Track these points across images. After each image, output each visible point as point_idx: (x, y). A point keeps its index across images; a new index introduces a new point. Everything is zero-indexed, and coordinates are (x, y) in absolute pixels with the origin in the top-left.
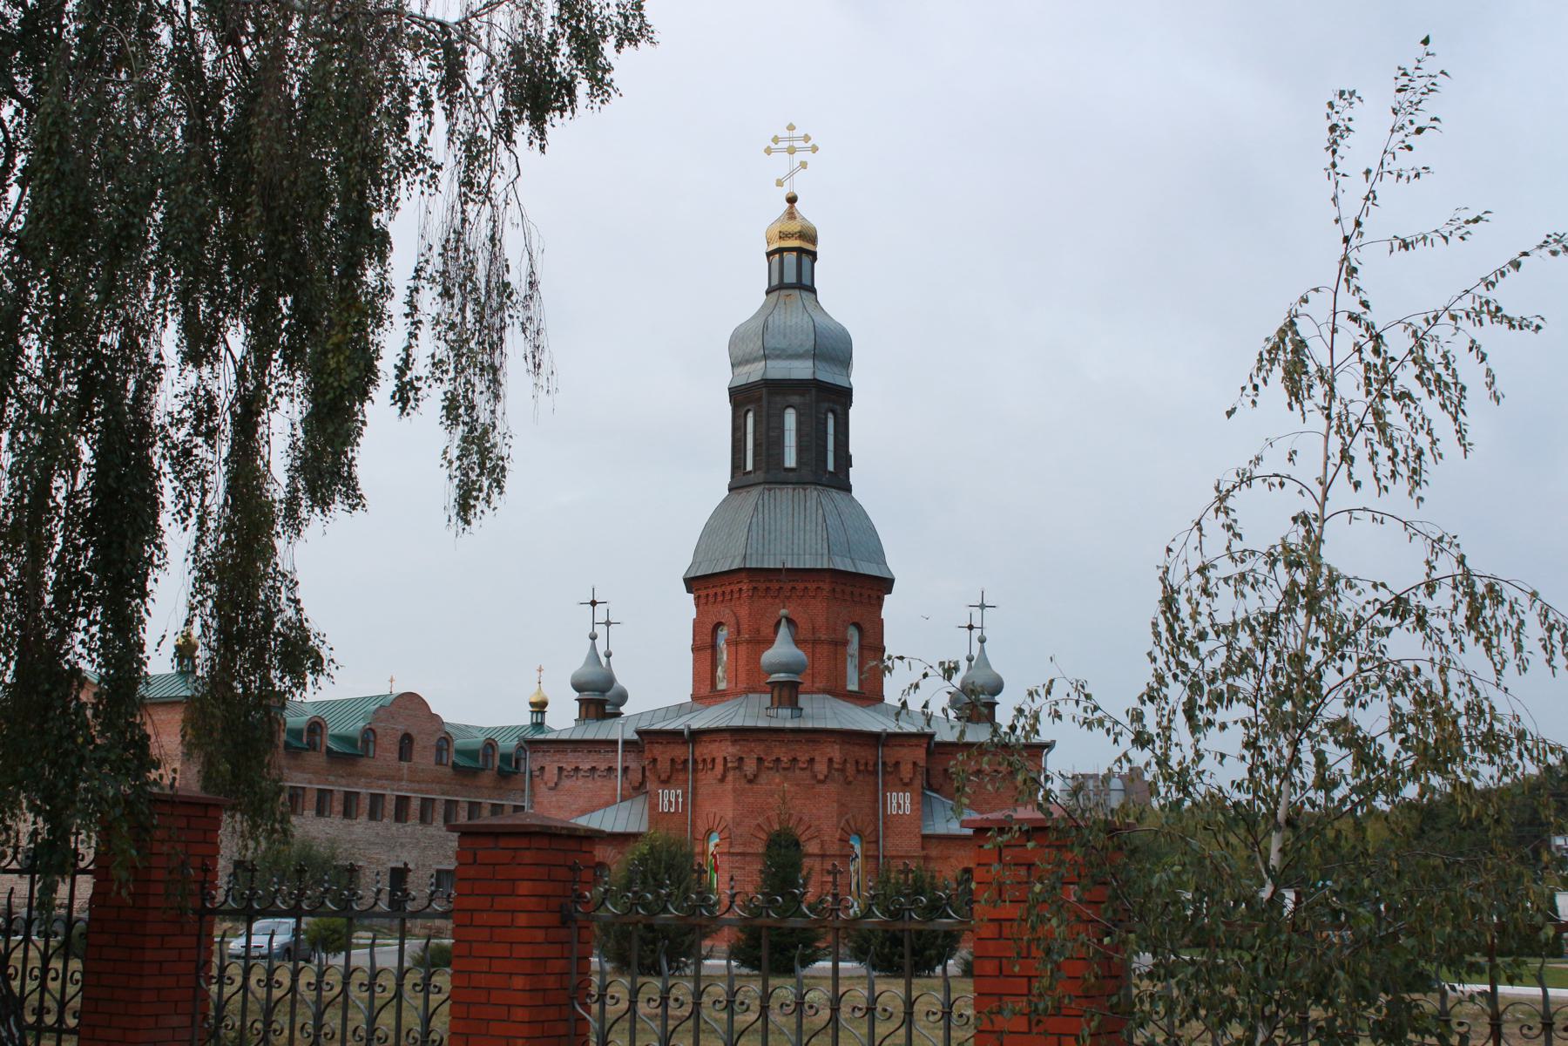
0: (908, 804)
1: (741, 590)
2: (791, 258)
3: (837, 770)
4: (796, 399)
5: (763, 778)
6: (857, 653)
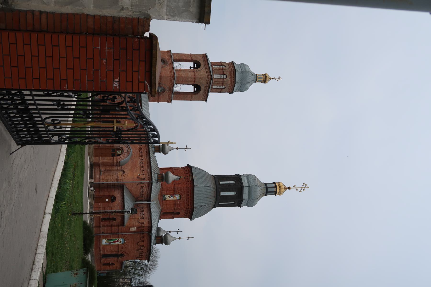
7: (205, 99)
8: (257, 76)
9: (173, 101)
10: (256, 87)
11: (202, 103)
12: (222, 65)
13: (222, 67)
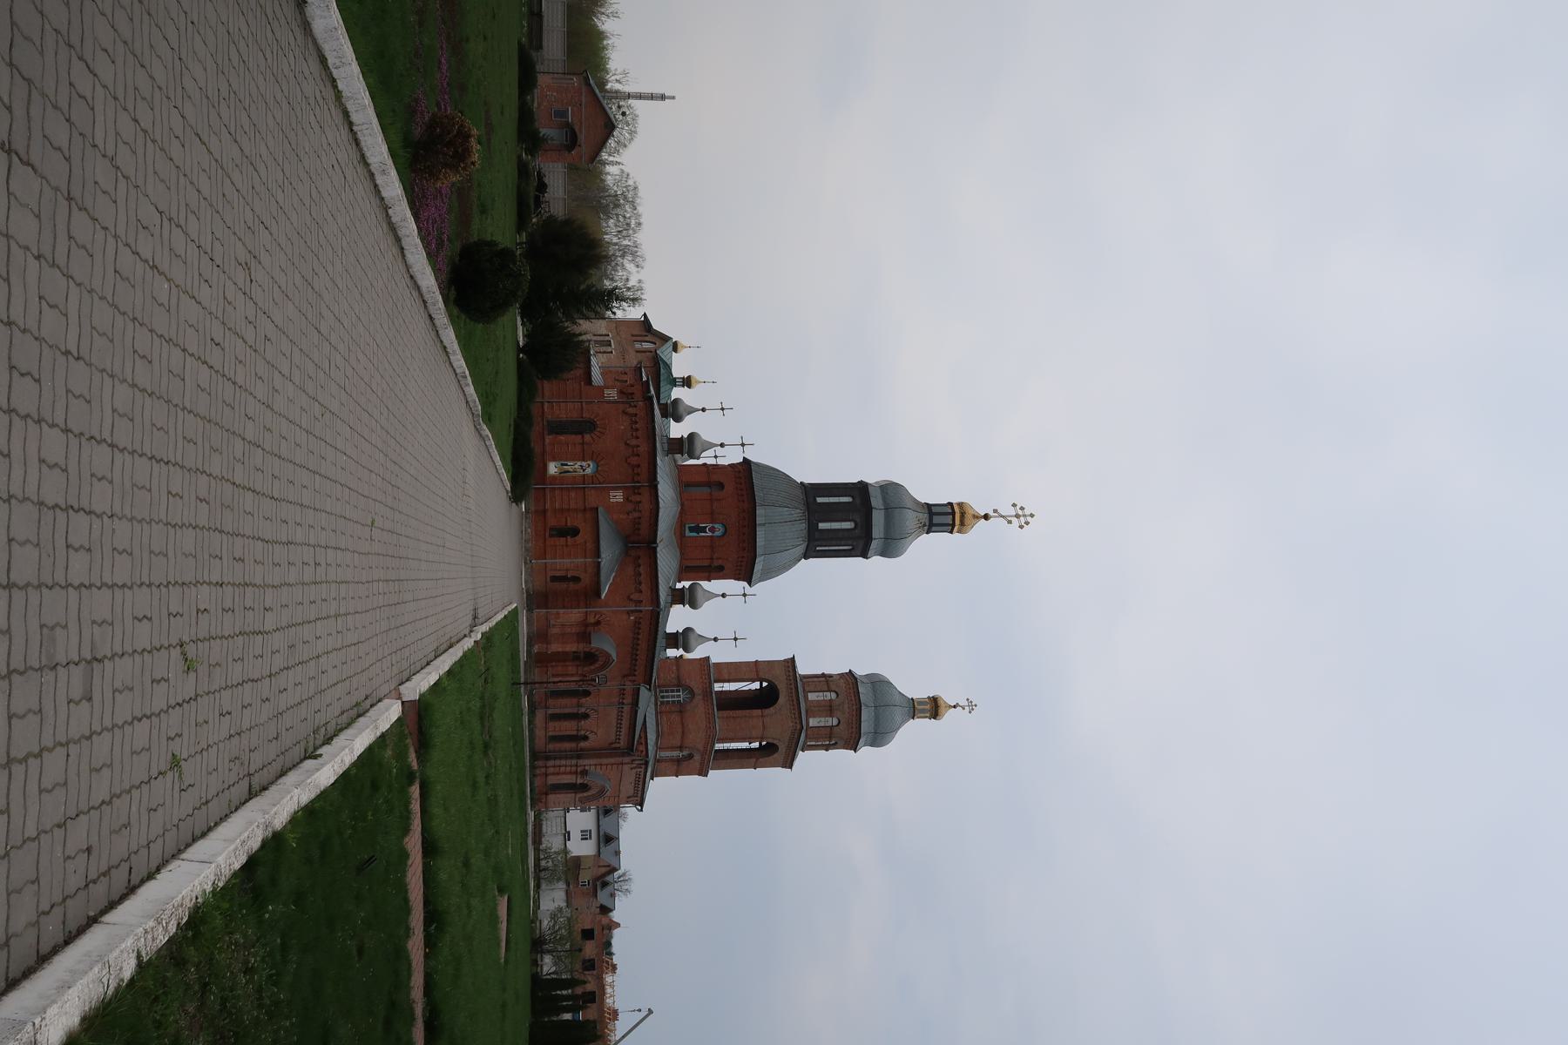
0: (615, 500)
1: (741, 484)
2: (949, 519)
3: (633, 451)
4: (858, 501)
8: (916, 706)
10: (913, 731)
11: (779, 772)
12: (830, 691)
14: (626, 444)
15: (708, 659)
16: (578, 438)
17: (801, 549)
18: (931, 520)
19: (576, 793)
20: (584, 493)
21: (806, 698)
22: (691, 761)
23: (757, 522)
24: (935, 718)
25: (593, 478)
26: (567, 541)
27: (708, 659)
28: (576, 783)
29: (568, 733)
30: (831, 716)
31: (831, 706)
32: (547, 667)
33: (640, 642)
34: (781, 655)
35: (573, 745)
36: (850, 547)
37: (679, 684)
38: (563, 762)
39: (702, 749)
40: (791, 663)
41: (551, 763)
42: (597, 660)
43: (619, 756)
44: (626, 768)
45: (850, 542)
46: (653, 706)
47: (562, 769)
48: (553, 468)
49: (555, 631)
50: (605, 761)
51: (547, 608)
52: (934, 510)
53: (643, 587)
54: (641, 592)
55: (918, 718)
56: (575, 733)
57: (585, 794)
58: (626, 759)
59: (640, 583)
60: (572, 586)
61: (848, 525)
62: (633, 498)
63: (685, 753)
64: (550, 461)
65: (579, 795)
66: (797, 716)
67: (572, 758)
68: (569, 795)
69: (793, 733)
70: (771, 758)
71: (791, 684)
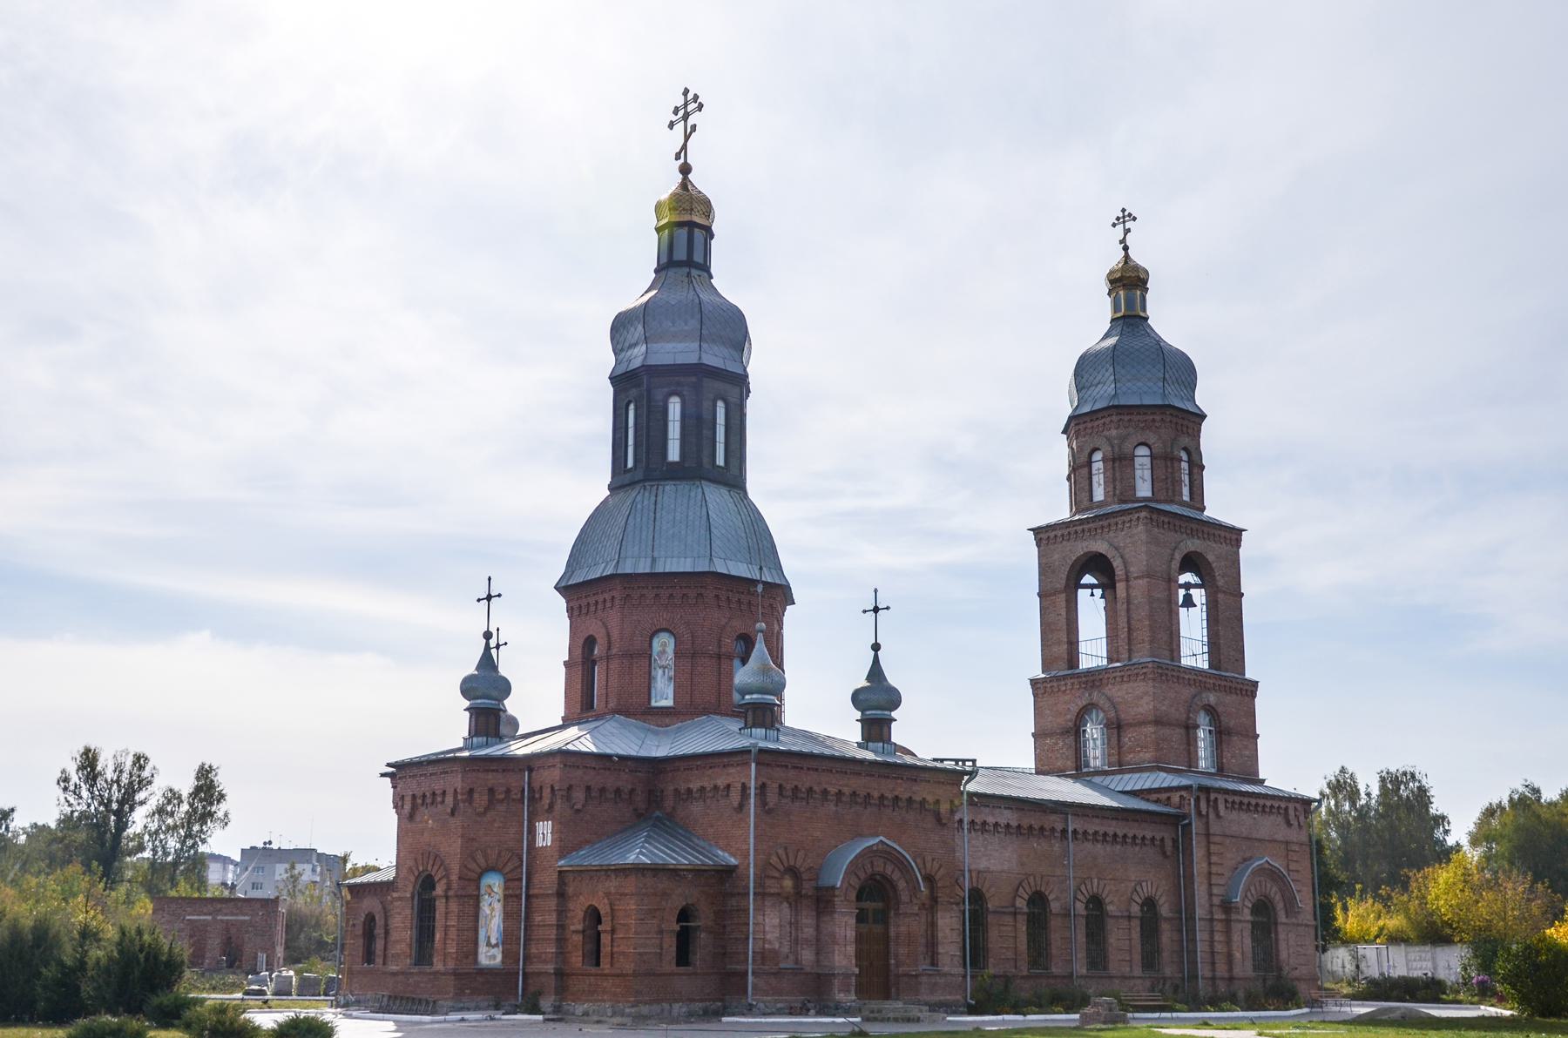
0: (549, 835)
3: (464, 801)
4: (633, 392)
5: (418, 818)
6: (671, 663)
7: (1233, 536)
8: (1119, 315)
9: (1250, 674)
11: (1247, 551)
12: (1089, 463)
13: (1098, 466)
14: (453, 814)
15: (1034, 683)
16: (440, 905)
17: (716, 496)
18: (680, 264)
19: (1276, 924)
20: (536, 896)
21: (1101, 504)
22: (1220, 709)
23: (647, 571)
24: (1145, 282)
25: (511, 881)
26: (605, 931)
27: (1034, 683)
28: (1252, 923)
29: (1136, 934)
30: (1132, 458)
31: (1114, 460)
32: (898, 976)
33: (846, 790)
34: (1029, 555)
35: (1165, 926)
36: (720, 404)
37: (1077, 731)
38: (1201, 948)
39: (1193, 690)
40: (1043, 535)
41: (1203, 970)
42: (884, 876)
43: (1192, 840)
44: (1215, 828)
45: (706, 404)
46: (1109, 778)
47: (1219, 948)
48: (490, 957)
49: (807, 956)
50: (1199, 866)
51: (746, 973)
52: (664, 260)
53: (721, 782)
54: (728, 786)
55: (1144, 309)
56: (1136, 924)
57: (1280, 906)
58: (1196, 826)
59: (716, 788)
60: (704, 919)
61: (675, 407)
62: (546, 801)
63: (1203, 719)
64: (476, 960)
65: (1282, 918)
66: (1126, 518)
67: (1192, 931)
68: (1282, 936)
69: (1160, 525)
70: (1214, 565)
71: (1076, 532)
